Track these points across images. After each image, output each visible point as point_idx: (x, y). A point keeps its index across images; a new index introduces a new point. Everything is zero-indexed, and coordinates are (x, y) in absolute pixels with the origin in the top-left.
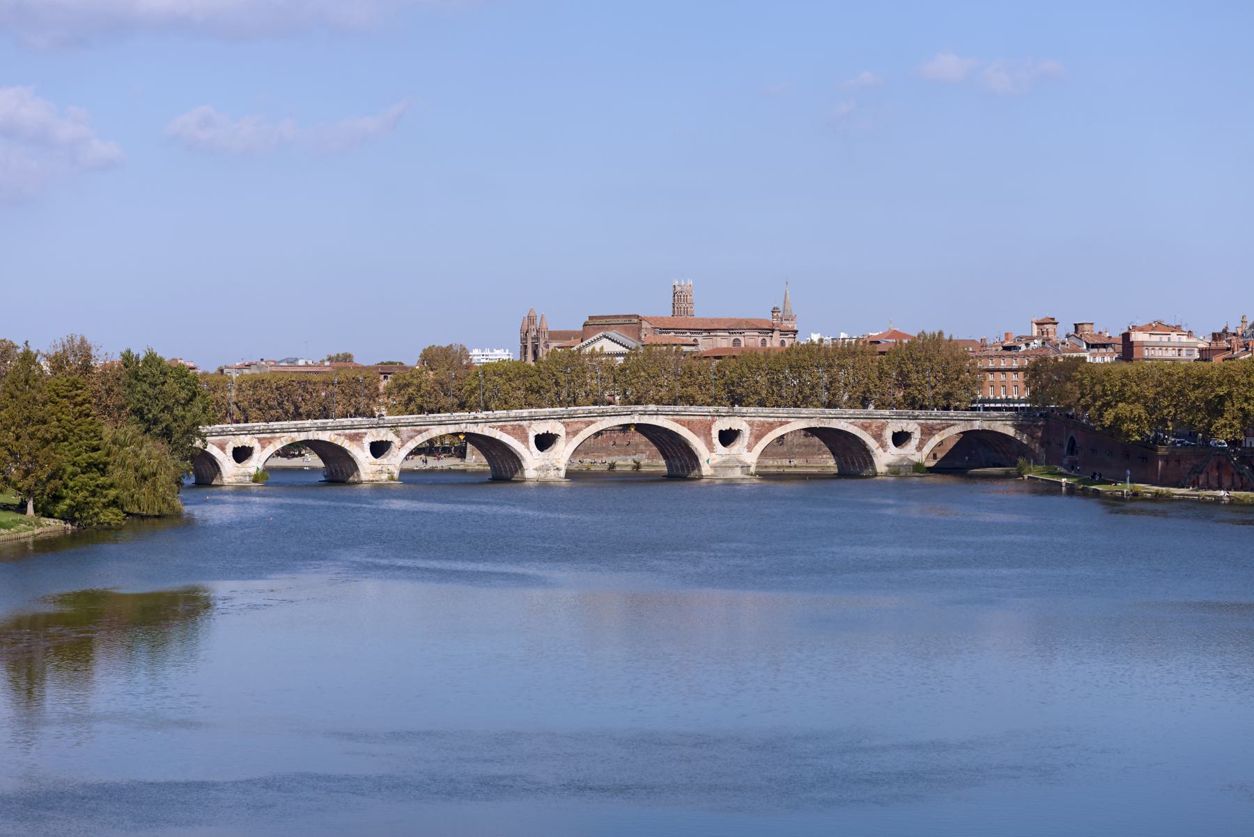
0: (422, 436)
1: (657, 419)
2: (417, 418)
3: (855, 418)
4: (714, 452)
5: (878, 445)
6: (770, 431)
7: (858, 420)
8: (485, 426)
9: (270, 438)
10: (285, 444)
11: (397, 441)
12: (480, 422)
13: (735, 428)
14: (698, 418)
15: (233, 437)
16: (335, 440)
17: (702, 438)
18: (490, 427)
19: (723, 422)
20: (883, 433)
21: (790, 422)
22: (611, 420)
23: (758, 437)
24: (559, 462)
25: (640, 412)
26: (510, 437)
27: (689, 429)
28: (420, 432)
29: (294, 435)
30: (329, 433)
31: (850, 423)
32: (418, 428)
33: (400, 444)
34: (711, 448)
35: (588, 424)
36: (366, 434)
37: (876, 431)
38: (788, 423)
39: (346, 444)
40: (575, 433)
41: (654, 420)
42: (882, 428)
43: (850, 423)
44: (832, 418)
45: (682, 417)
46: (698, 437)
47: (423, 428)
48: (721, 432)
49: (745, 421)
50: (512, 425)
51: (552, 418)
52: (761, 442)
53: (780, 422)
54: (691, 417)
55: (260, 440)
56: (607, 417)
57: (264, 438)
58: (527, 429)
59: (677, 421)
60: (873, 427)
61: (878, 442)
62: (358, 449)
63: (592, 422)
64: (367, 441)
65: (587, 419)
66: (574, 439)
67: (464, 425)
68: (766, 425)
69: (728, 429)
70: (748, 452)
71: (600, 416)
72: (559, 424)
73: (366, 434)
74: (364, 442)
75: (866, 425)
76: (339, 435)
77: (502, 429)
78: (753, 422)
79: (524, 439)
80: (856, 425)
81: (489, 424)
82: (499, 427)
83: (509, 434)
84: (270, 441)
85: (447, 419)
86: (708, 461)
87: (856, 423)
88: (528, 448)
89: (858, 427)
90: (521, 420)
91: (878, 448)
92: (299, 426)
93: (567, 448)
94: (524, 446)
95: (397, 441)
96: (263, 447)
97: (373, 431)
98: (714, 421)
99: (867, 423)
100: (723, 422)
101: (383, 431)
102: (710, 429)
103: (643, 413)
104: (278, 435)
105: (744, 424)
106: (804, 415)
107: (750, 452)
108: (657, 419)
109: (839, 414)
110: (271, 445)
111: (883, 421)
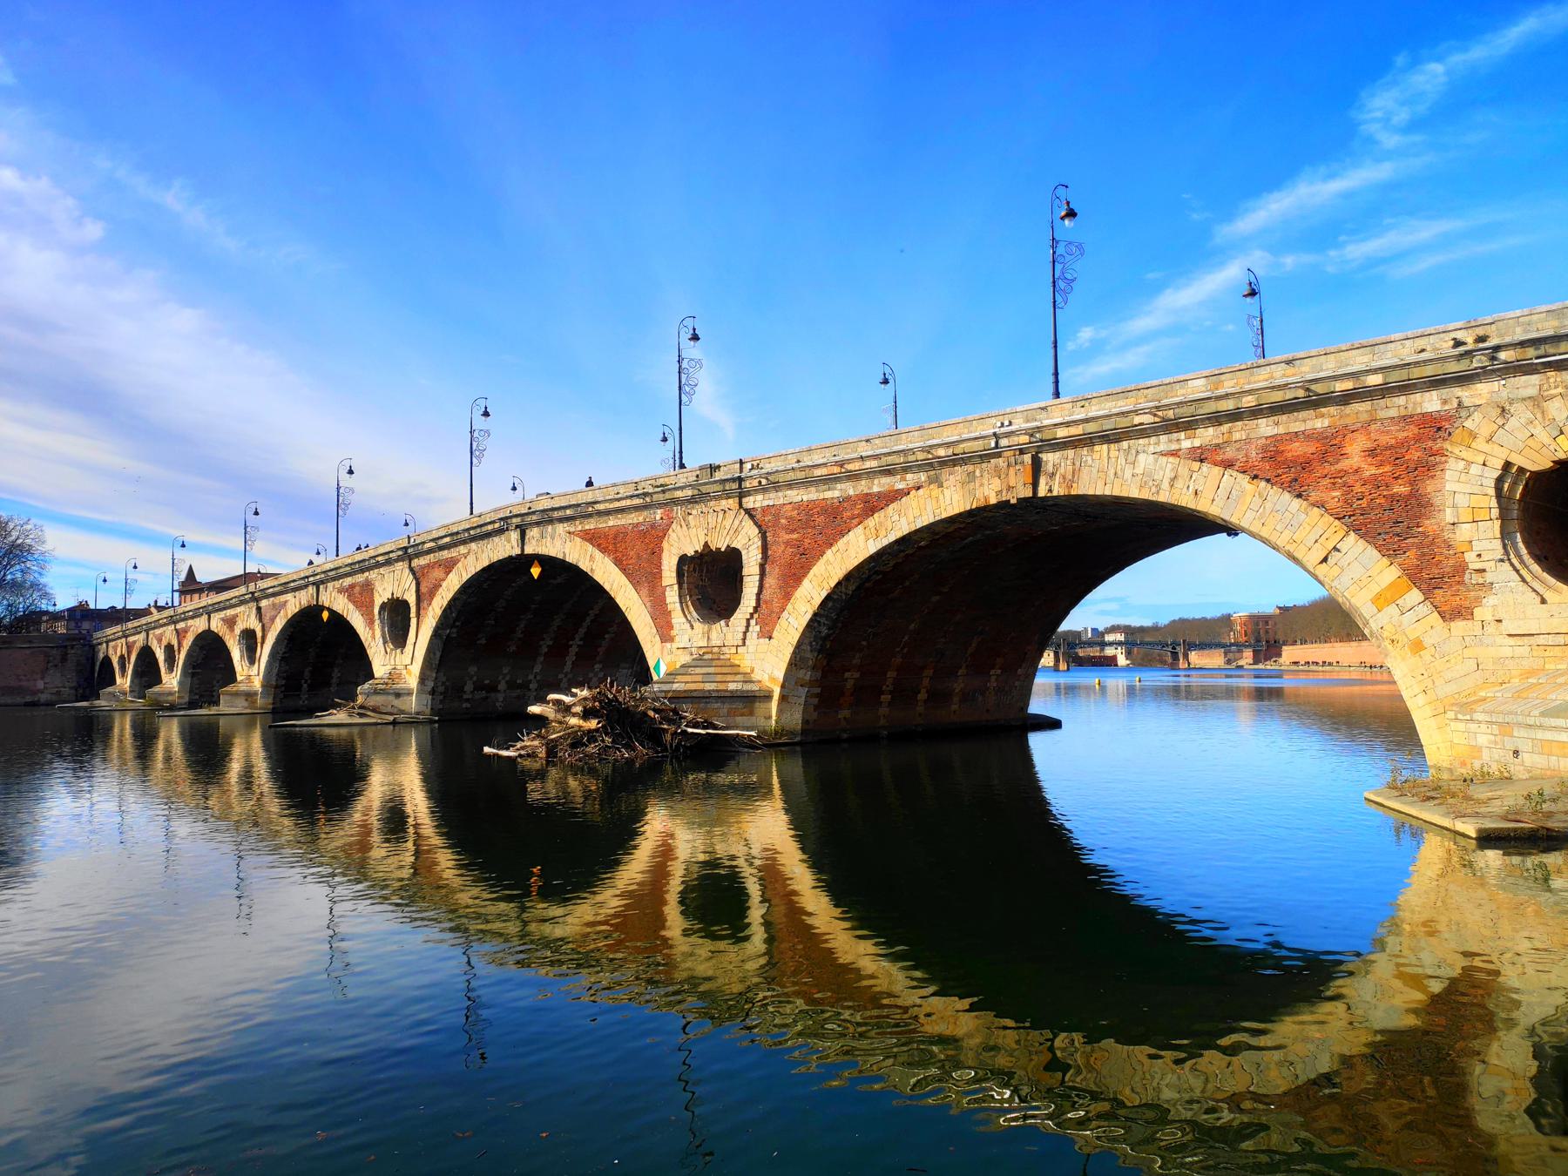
4: (671, 640)
5: (1388, 573)
7: (1239, 431)
13: (720, 543)
17: (645, 591)
20: (1430, 487)
24: (409, 673)
35: (449, 566)
37: (1376, 483)
38: (893, 496)
46: (636, 584)
56: (473, 545)
60: (1354, 454)
61: (1390, 552)
64: (237, 631)
67: (310, 588)
68: (820, 520)
69: (699, 548)
75: (1298, 449)
80: (1228, 465)
87: (1230, 453)
99: (1308, 436)
111: (1431, 402)
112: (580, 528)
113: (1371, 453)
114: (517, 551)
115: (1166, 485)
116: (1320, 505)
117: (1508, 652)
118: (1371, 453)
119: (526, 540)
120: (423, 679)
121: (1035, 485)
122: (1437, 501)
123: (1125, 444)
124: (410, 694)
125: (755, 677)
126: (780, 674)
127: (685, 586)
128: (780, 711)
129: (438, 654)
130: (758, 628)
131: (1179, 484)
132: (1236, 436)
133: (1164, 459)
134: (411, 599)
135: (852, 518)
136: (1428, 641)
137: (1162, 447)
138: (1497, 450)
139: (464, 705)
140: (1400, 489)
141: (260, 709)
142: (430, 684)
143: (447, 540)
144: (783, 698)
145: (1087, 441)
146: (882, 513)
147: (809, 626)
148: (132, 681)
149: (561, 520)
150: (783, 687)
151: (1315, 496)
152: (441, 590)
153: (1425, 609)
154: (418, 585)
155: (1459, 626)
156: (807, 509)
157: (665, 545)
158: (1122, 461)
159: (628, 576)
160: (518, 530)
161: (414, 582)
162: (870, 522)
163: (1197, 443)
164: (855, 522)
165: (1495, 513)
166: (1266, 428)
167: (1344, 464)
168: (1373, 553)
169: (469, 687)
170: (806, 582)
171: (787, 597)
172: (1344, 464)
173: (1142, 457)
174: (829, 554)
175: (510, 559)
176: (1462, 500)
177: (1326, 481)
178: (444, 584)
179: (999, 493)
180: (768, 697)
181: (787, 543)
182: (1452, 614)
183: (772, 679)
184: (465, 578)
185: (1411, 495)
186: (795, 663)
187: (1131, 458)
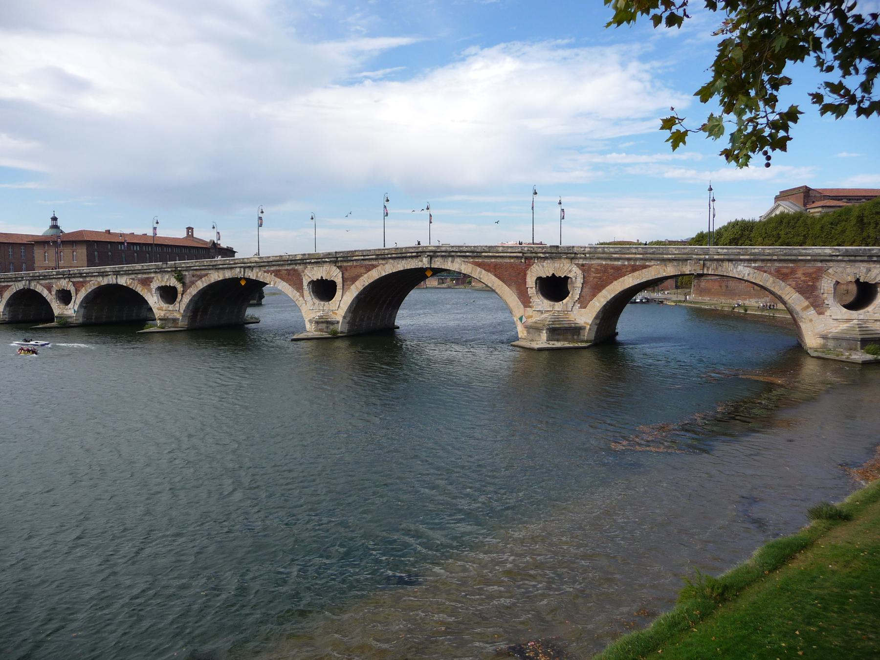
0: (202, 281)
1: (452, 262)
2: (196, 262)
3: (763, 260)
4: (530, 307)
6: (616, 280)
8: (260, 270)
9: (81, 282)
10: (93, 288)
11: (179, 287)
12: (254, 266)
13: (561, 274)
14: (508, 260)
15: (56, 280)
16: (131, 284)
18: (265, 272)
19: (543, 266)
20: (817, 284)
21: (649, 266)
22: (396, 263)
23: (598, 288)
25: (428, 253)
26: (285, 283)
27: (496, 275)
28: (200, 277)
29: (100, 279)
30: (125, 278)
31: (755, 268)
32: (198, 273)
33: (182, 289)
34: (526, 301)
35: (369, 268)
36: (153, 278)
37: (804, 281)
38: (645, 267)
39: (139, 289)
40: (354, 279)
41: (449, 262)
42: (816, 277)
43: (755, 268)
44: (723, 260)
45: (486, 260)
46: (509, 286)
47: (203, 272)
48: (539, 279)
49: (575, 264)
50: (287, 270)
51: (327, 262)
52: (600, 294)
53: (633, 266)
54: (499, 260)
55: (74, 284)
56: (391, 261)
57: (79, 282)
58: (302, 274)
59: (479, 265)
60: (799, 274)
61: (807, 298)
62: (149, 293)
63: (374, 266)
64: (154, 285)
65: (367, 262)
66: (352, 287)
67: (238, 270)
70: (580, 308)
71: (381, 259)
72: (335, 268)
73: (153, 278)
74: (152, 287)
75: (785, 271)
76: (133, 279)
77: (277, 274)
78: (590, 266)
79: (299, 287)
81: (263, 269)
82: (273, 271)
83: (283, 279)
84: (83, 284)
85: (222, 263)
86: (521, 319)
87: (766, 269)
88: (303, 297)
89: (770, 273)
90: (296, 264)
91: (807, 307)
92: (102, 270)
93: (344, 297)
94: (298, 294)
95: (179, 287)
96: (77, 291)
97: (159, 276)
98: (528, 266)
99: (787, 267)
100: (543, 266)
101: (167, 276)
102: (525, 275)
103: (431, 254)
104: (88, 279)
105: (575, 269)
106: (670, 256)
107: (585, 308)
108: (452, 262)
109: (733, 254)
110: (84, 288)
111: (819, 264)
112: (472, 260)
113: (804, 274)
114: (428, 266)
115: (746, 275)
116: (790, 285)
117: (832, 322)
118: (804, 274)
119: (433, 262)
120: (344, 317)
121: (703, 270)
122: (819, 287)
123: (734, 262)
124: (338, 322)
125: (576, 322)
126: (590, 322)
127: (537, 288)
128: (588, 333)
129: (354, 305)
130: (579, 305)
131: (751, 276)
132: (768, 265)
133: (746, 268)
134: (339, 280)
135: (627, 271)
136: (813, 319)
137: (745, 265)
138: (835, 278)
139: (356, 328)
140: (810, 283)
141: (587, 342)
142: (348, 319)
143: (374, 257)
144: (590, 329)
145: (723, 260)
146: (640, 271)
147: (604, 306)
148: (5, 309)
149: (460, 256)
150: (590, 325)
151: (788, 283)
152: (361, 278)
153: (814, 312)
154: (342, 274)
155: (821, 316)
156: (606, 267)
157: (529, 272)
158: (732, 266)
159: (503, 281)
160: (429, 257)
161: (341, 273)
162: (636, 274)
163: (756, 265)
164: (628, 273)
165: (833, 292)
166: (777, 264)
167: (796, 276)
168: (802, 298)
169: (357, 320)
170: (604, 291)
171: (594, 295)
172: (796, 276)
173: (739, 266)
174: (615, 283)
175: (421, 269)
176: (826, 288)
177: (792, 279)
178: (366, 276)
179: (690, 271)
180: (584, 328)
181: (595, 277)
182: (821, 313)
183: (585, 323)
184: (384, 274)
185: (812, 285)
186: (596, 318)
187: (736, 266)
